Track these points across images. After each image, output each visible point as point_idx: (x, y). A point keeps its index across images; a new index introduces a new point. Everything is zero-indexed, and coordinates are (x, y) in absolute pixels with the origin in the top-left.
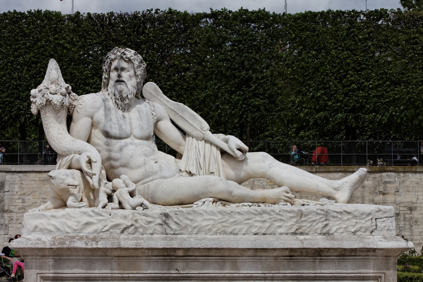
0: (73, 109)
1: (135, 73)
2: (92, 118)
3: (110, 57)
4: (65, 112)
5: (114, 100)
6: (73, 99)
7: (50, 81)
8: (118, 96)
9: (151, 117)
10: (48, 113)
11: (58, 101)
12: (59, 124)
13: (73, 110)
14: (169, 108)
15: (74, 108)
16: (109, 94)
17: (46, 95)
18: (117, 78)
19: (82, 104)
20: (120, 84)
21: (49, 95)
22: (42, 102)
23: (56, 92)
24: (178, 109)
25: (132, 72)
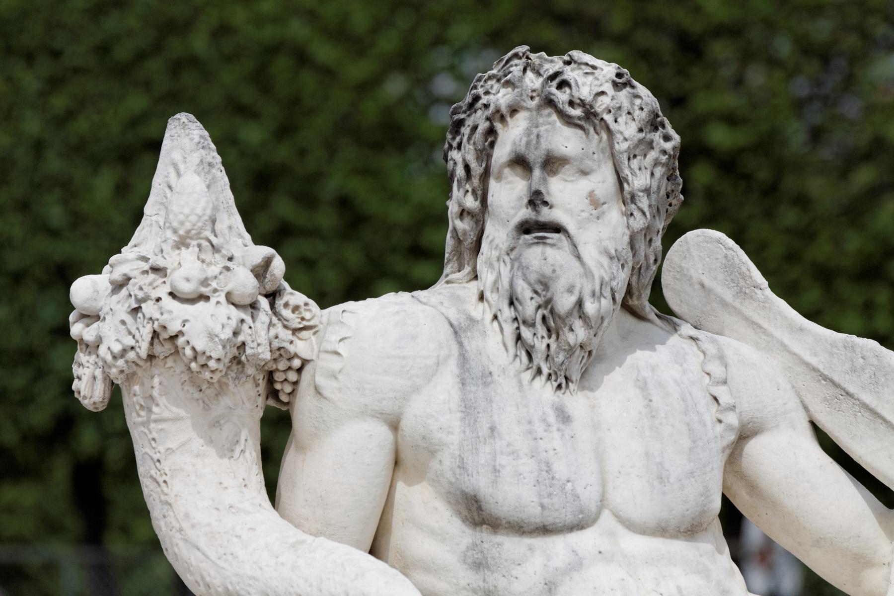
0: (292, 376)
1: (621, 181)
2: (395, 426)
3: (484, 100)
4: (253, 393)
5: (510, 329)
6: (296, 323)
7: (169, 234)
8: (529, 308)
9: (710, 412)
10: (162, 401)
11: (212, 336)
12: (222, 456)
13: (296, 383)
14: (807, 364)
15: (299, 371)
16: (482, 297)
17: (149, 308)
18: (525, 213)
20: (542, 241)
21: (168, 302)
22: (129, 341)
24: (853, 370)
25: (603, 180)
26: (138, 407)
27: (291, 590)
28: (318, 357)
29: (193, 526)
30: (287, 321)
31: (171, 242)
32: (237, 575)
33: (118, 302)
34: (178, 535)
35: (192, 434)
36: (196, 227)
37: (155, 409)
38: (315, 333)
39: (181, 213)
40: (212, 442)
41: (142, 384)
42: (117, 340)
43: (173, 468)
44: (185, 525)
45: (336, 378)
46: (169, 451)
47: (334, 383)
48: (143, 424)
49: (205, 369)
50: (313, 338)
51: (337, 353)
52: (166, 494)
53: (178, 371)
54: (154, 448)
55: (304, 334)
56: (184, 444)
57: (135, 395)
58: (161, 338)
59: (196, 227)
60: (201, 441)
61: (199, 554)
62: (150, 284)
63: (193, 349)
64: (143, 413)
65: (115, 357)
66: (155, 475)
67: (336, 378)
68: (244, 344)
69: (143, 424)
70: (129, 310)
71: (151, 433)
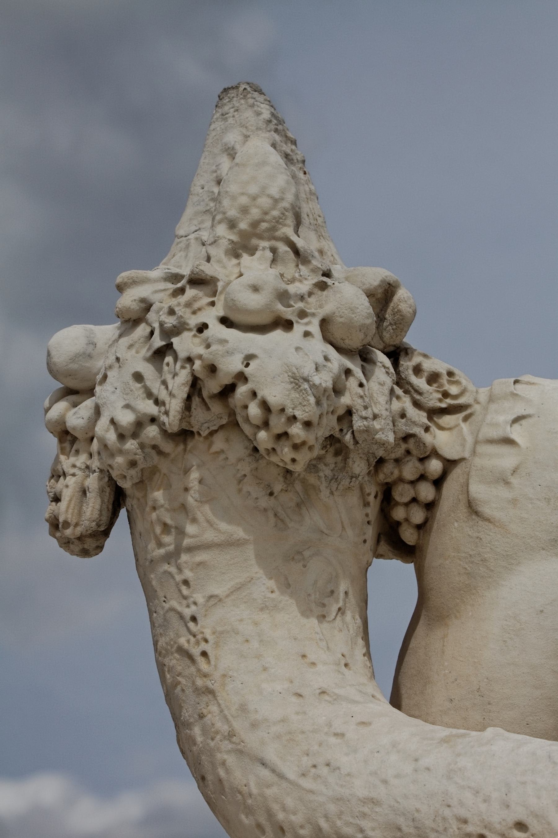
0: (426, 492)
4: (359, 514)
6: (433, 399)
7: (222, 230)
11: (298, 380)
12: (306, 613)
13: (430, 506)
15: (438, 483)
17: (184, 344)
19: (516, 433)
21: (217, 330)
22: (149, 408)
23: (288, 313)
26: (158, 530)
27: (447, 812)
28: (474, 452)
29: (254, 725)
30: (420, 394)
31: (224, 244)
32: (338, 800)
33: (130, 347)
34: (226, 745)
35: (256, 571)
36: (268, 217)
37: (190, 529)
38: (466, 419)
39: (243, 194)
40: (288, 586)
41: (168, 487)
42: (127, 406)
43: (219, 629)
44: (237, 725)
45: (507, 483)
46: (212, 602)
47: (503, 493)
48: (169, 558)
49: (283, 441)
50: (465, 427)
51: (508, 441)
52: (205, 676)
53: (232, 457)
54: (185, 598)
55: (447, 420)
56: (238, 588)
57: (154, 508)
58: (205, 394)
59: (268, 217)
60: (272, 584)
61: (265, 773)
62: (188, 305)
63: (265, 406)
64: (167, 539)
65: (121, 437)
66: (186, 646)
67: (507, 483)
68: (349, 412)
69: (169, 558)
70: (150, 353)
71: (180, 570)
